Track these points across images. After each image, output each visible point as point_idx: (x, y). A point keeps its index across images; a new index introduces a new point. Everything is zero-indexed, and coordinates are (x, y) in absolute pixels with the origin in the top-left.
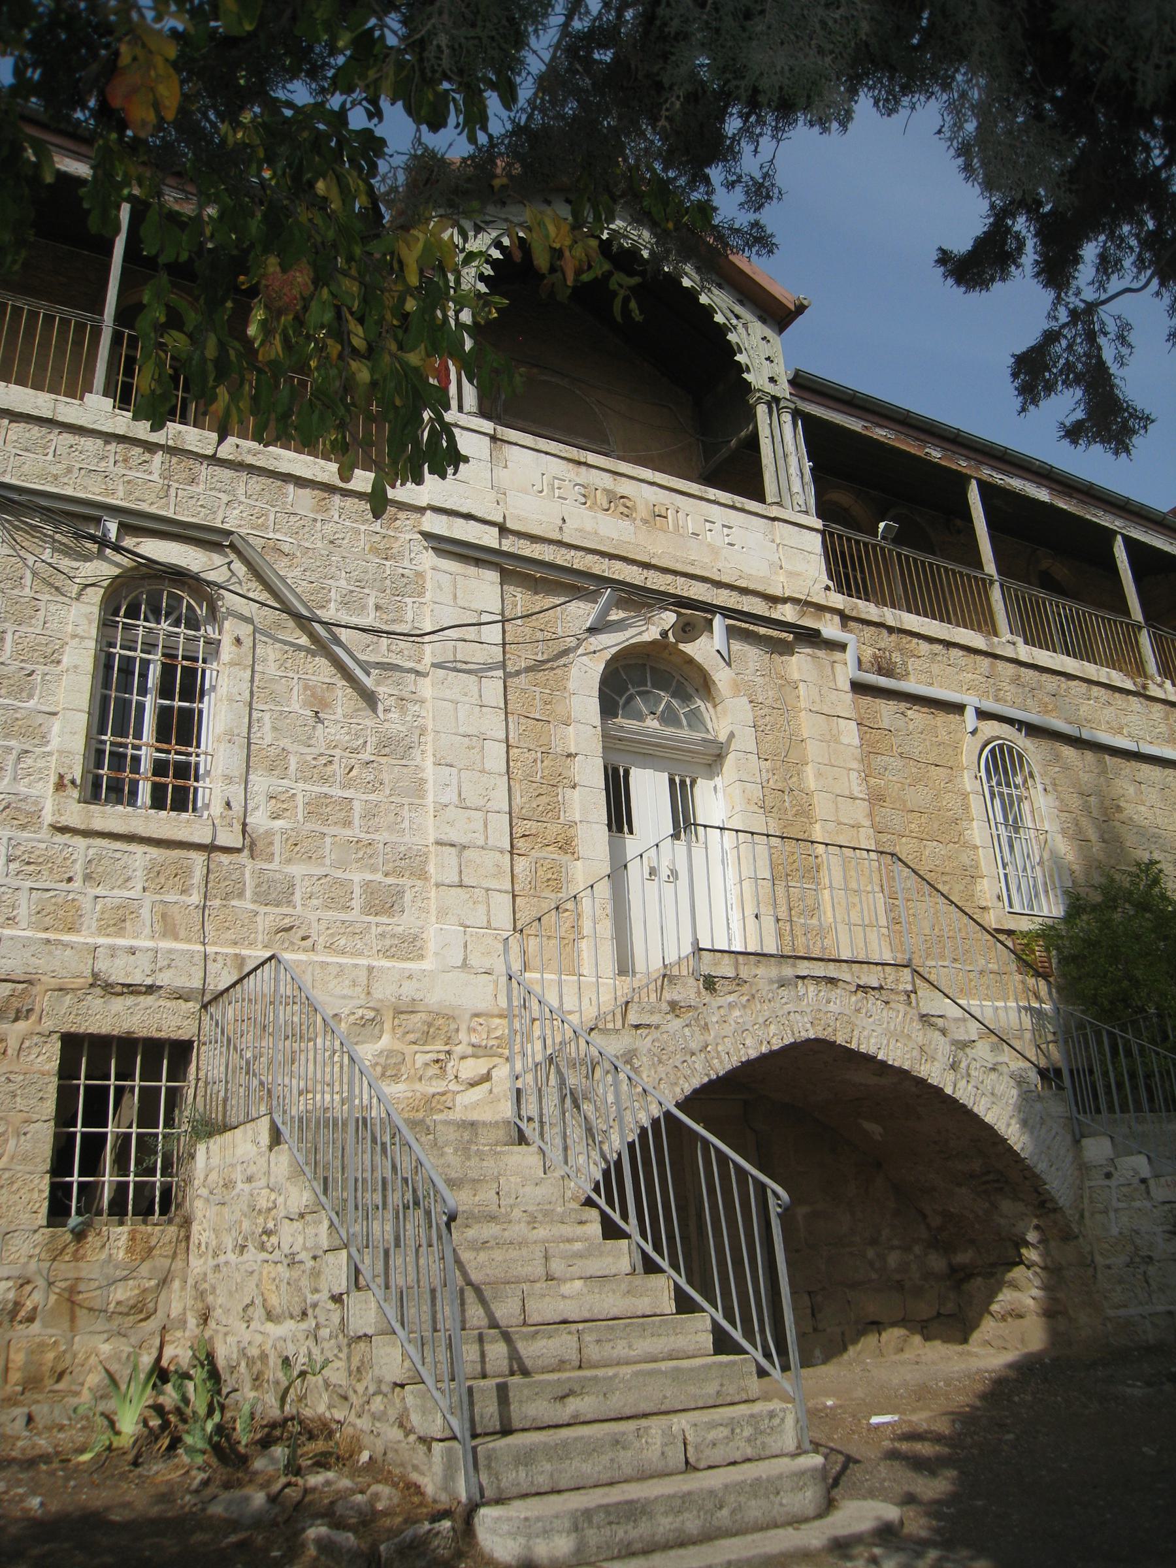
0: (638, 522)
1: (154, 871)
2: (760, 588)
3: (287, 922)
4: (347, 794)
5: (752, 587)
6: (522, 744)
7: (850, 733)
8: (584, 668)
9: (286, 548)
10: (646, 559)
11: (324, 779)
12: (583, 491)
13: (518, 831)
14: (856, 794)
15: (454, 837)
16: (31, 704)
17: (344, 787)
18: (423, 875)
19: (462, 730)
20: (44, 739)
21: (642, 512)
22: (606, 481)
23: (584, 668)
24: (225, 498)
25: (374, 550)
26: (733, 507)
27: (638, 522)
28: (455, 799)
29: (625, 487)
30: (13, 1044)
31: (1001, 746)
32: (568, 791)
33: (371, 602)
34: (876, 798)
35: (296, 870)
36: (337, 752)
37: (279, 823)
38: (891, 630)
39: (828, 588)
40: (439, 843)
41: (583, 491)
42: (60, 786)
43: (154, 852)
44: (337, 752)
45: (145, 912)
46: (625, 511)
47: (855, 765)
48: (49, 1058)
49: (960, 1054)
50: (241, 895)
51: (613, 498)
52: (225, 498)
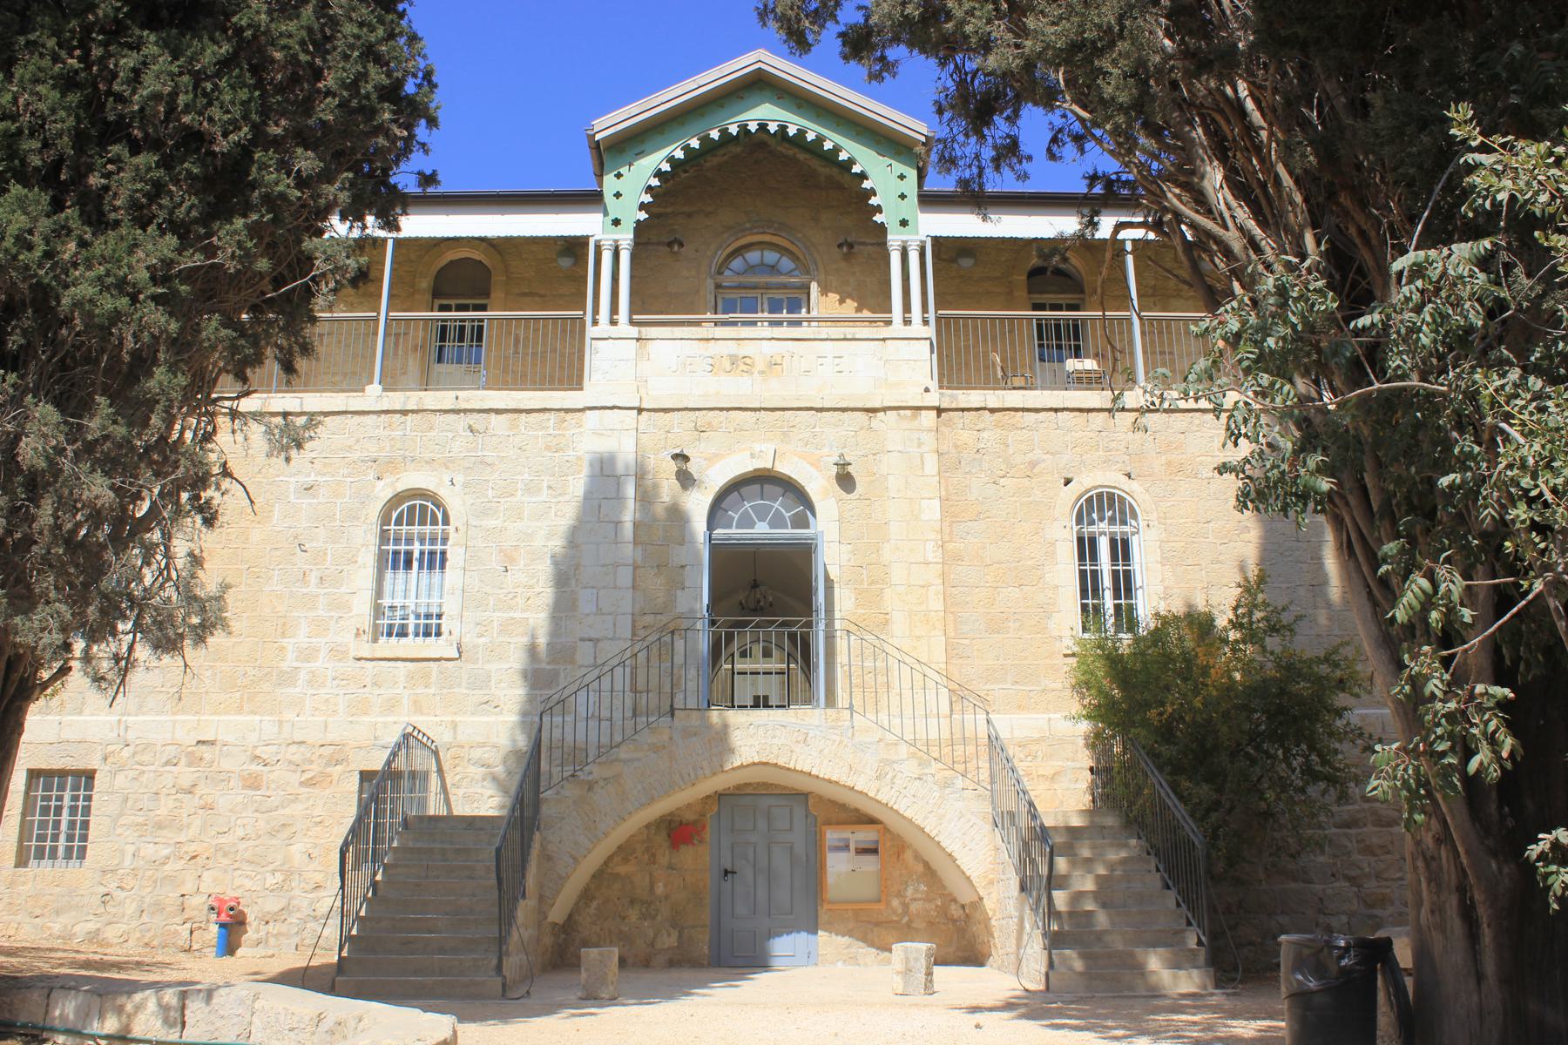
0: (756, 375)
1: (410, 677)
2: (860, 405)
3: (486, 699)
4: (526, 615)
5: (852, 405)
7: (931, 510)
9: (489, 460)
10: (757, 405)
11: (511, 608)
12: (710, 361)
13: (639, 625)
15: (593, 635)
16: (343, 589)
17: (523, 611)
18: (572, 661)
20: (350, 609)
21: (760, 365)
22: (732, 347)
24: (450, 435)
25: (548, 448)
27: (756, 375)
29: (747, 349)
30: (335, 778)
31: (1100, 495)
32: (679, 592)
33: (545, 485)
34: (950, 560)
35: (492, 667)
36: (520, 590)
37: (483, 640)
38: (992, 411)
39: (927, 390)
40: (582, 640)
41: (710, 361)
42: (357, 635)
43: (408, 664)
44: (520, 590)
45: (405, 701)
46: (745, 368)
47: (933, 536)
48: (354, 782)
49: (887, 768)
50: (459, 685)
51: (734, 360)
52: (450, 435)
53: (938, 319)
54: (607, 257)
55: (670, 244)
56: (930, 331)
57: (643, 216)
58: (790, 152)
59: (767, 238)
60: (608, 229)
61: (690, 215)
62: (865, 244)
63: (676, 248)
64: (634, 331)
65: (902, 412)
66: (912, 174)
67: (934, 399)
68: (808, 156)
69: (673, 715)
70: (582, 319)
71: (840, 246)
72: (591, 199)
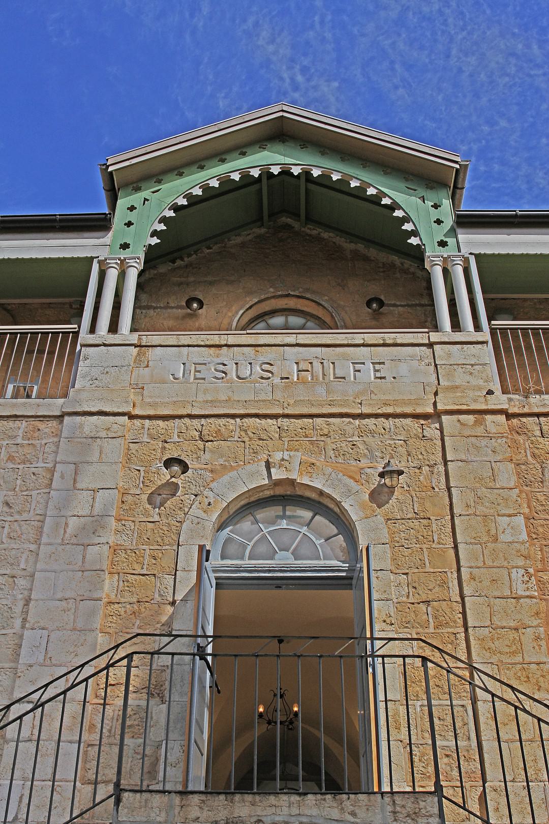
6: (123, 600)
8: (196, 520)
12: (221, 367)
14: (521, 592)
19: (59, 595)
23: (196, 520)
26: (385, 345)
27: (277, 380)
28: (41, 659)
39: (490, 392)
41: (221, 367)
47: (521, 562)
53: (493, 332)
54: (112, 275)
55: (189, 303)
56: (486, 335)
57: (155, 241)
58: (314, 232)
59: (291, 303)
60: (118, 254)
61: (211, 283)
62: (395, 305)
63: (195, 305)
64: (134, 338)
65: (463, 417)
66: (447, 203)
67: (500, 401)
68: (331, 234)
69: (118, 801)
70: (76, 334)
71: (369, 304)
72: (100, 224)
